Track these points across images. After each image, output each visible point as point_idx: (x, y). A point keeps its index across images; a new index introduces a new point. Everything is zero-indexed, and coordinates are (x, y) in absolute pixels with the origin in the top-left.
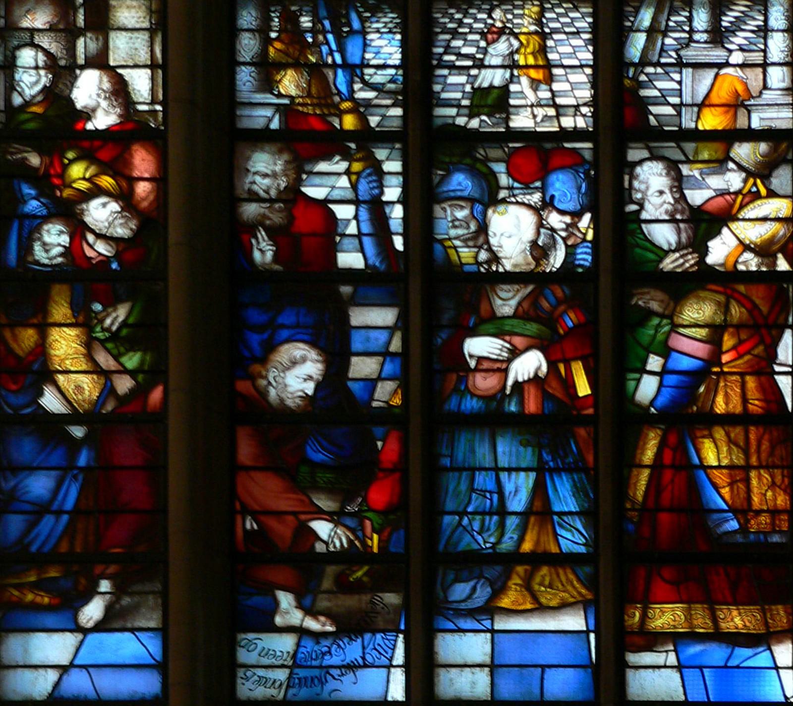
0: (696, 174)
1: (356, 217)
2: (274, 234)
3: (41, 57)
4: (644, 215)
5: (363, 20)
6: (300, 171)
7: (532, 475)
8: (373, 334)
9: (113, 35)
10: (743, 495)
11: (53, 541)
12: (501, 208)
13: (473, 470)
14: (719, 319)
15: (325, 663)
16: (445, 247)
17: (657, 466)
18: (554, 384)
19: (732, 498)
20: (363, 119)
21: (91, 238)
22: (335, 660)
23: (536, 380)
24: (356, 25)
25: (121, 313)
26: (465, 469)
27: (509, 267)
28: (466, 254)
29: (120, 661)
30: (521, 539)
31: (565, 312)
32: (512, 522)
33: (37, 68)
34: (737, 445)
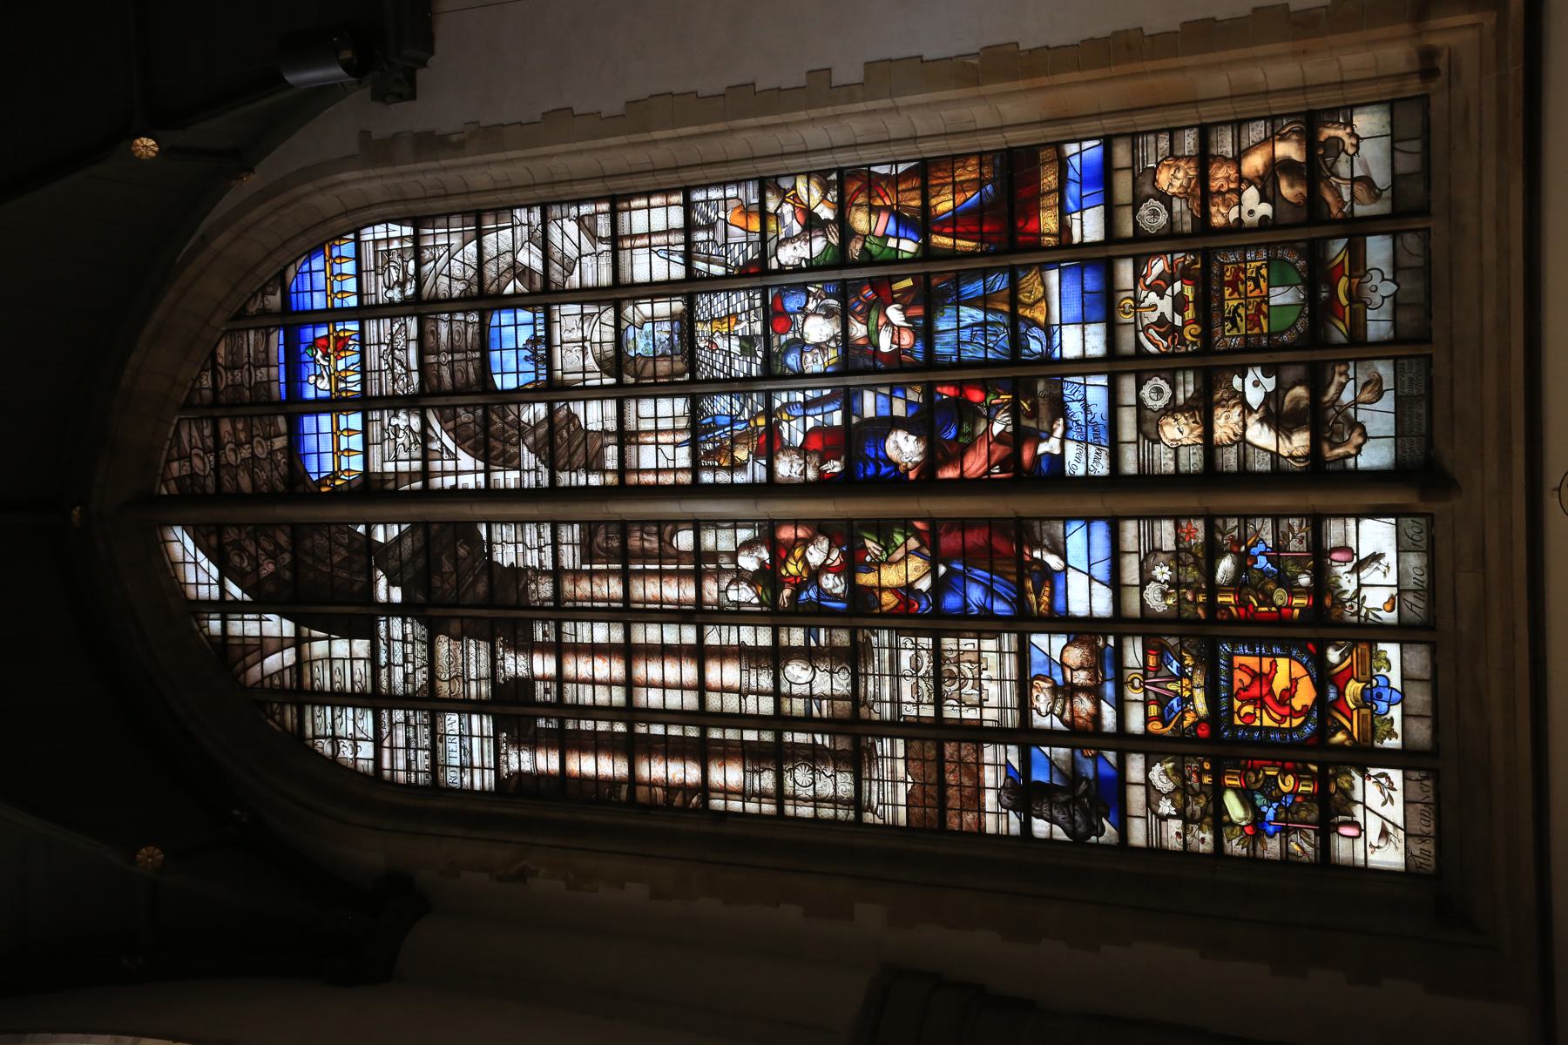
0: (784, 230)
1: (813, 416)
2: (823, 461)
3: (732, 587)
4: (808, 257)
5: (708, 416)
6: (788, 448)
7: (962, 308)
8: (879, 403)
9: (719, 549)
10: (971, 184)
11: (1009, 584)
12: (806, 336)
13: (959, 342)
14: (866, 209)
15: (1083, 423)
16: (829, 366)
17: (955, 236)
18: (906, 299)
19: (972, 190)
20: (759, 414)
21: (829, 562)
22: (1080, 417)
23: (903, 310)
24: (710, 420)
25: (869, 544)
26: (959, 348)
27: (839, 330)
28: (832, 354)
29: (1086, 546)
30: (1002, 312)
31: (863, 296)
32: (990, 318)
33: (738, 590)
34: (940, 191)
